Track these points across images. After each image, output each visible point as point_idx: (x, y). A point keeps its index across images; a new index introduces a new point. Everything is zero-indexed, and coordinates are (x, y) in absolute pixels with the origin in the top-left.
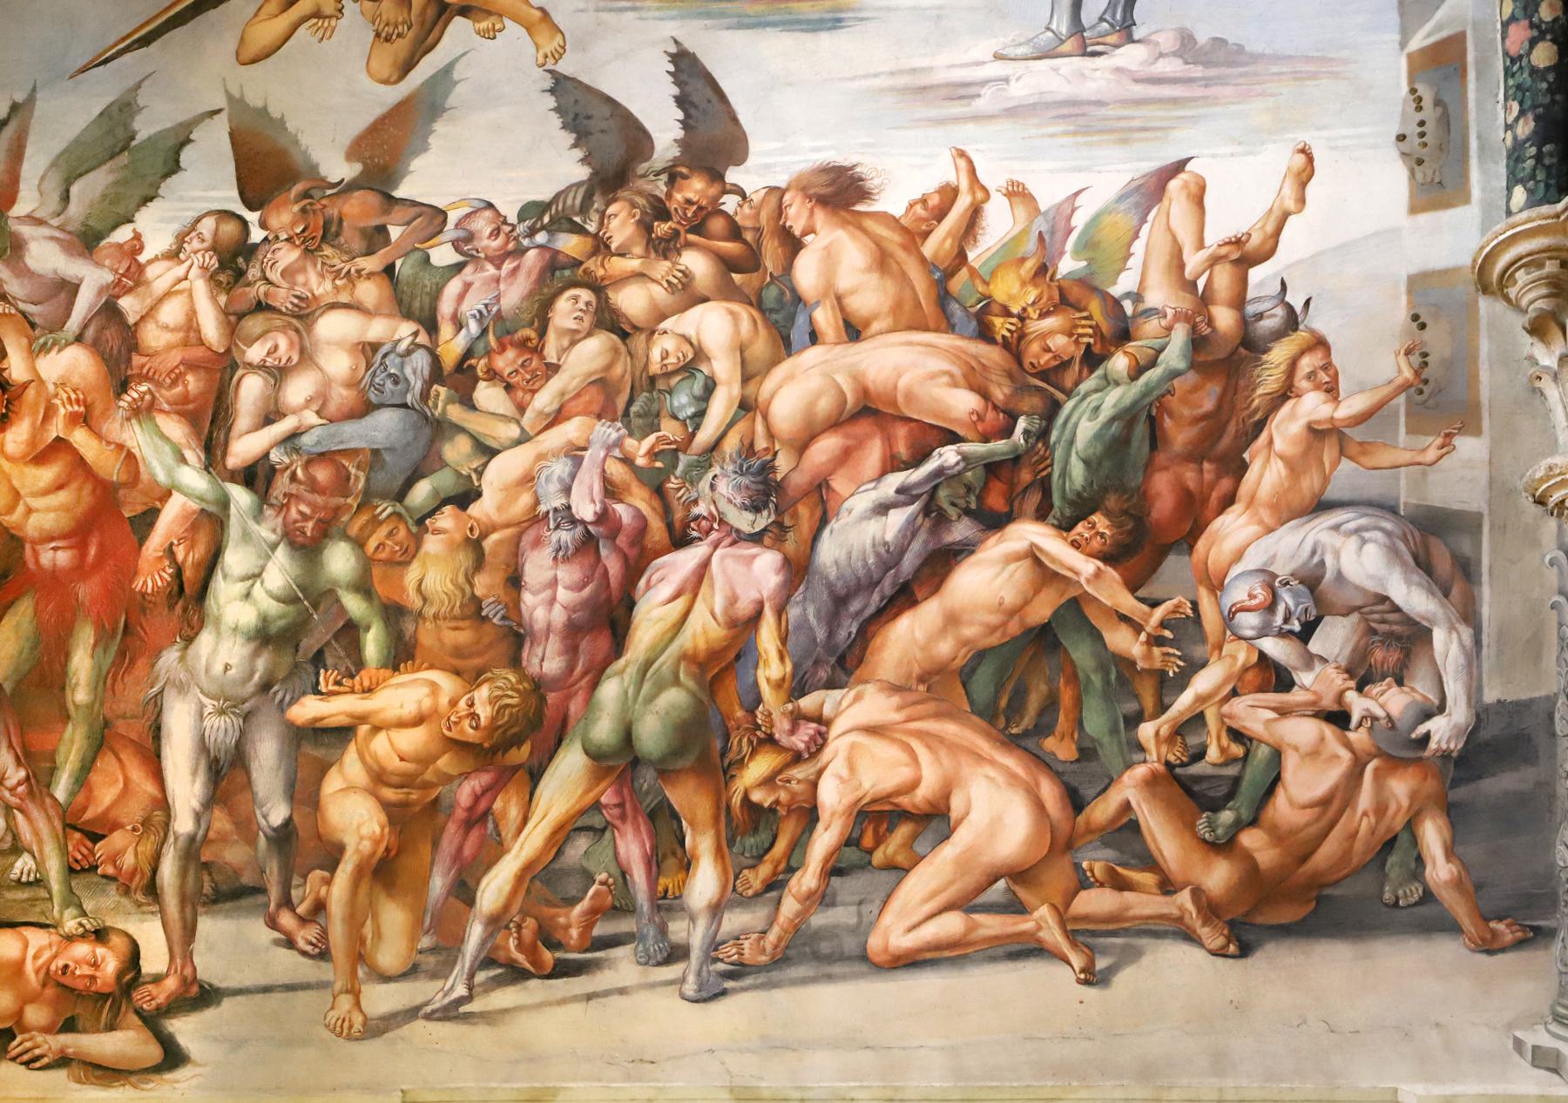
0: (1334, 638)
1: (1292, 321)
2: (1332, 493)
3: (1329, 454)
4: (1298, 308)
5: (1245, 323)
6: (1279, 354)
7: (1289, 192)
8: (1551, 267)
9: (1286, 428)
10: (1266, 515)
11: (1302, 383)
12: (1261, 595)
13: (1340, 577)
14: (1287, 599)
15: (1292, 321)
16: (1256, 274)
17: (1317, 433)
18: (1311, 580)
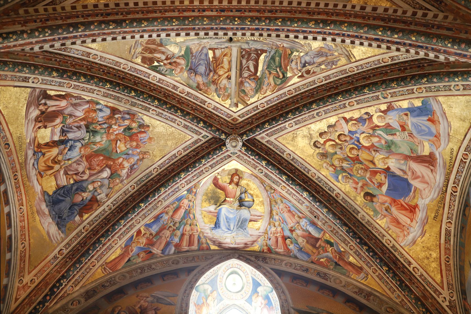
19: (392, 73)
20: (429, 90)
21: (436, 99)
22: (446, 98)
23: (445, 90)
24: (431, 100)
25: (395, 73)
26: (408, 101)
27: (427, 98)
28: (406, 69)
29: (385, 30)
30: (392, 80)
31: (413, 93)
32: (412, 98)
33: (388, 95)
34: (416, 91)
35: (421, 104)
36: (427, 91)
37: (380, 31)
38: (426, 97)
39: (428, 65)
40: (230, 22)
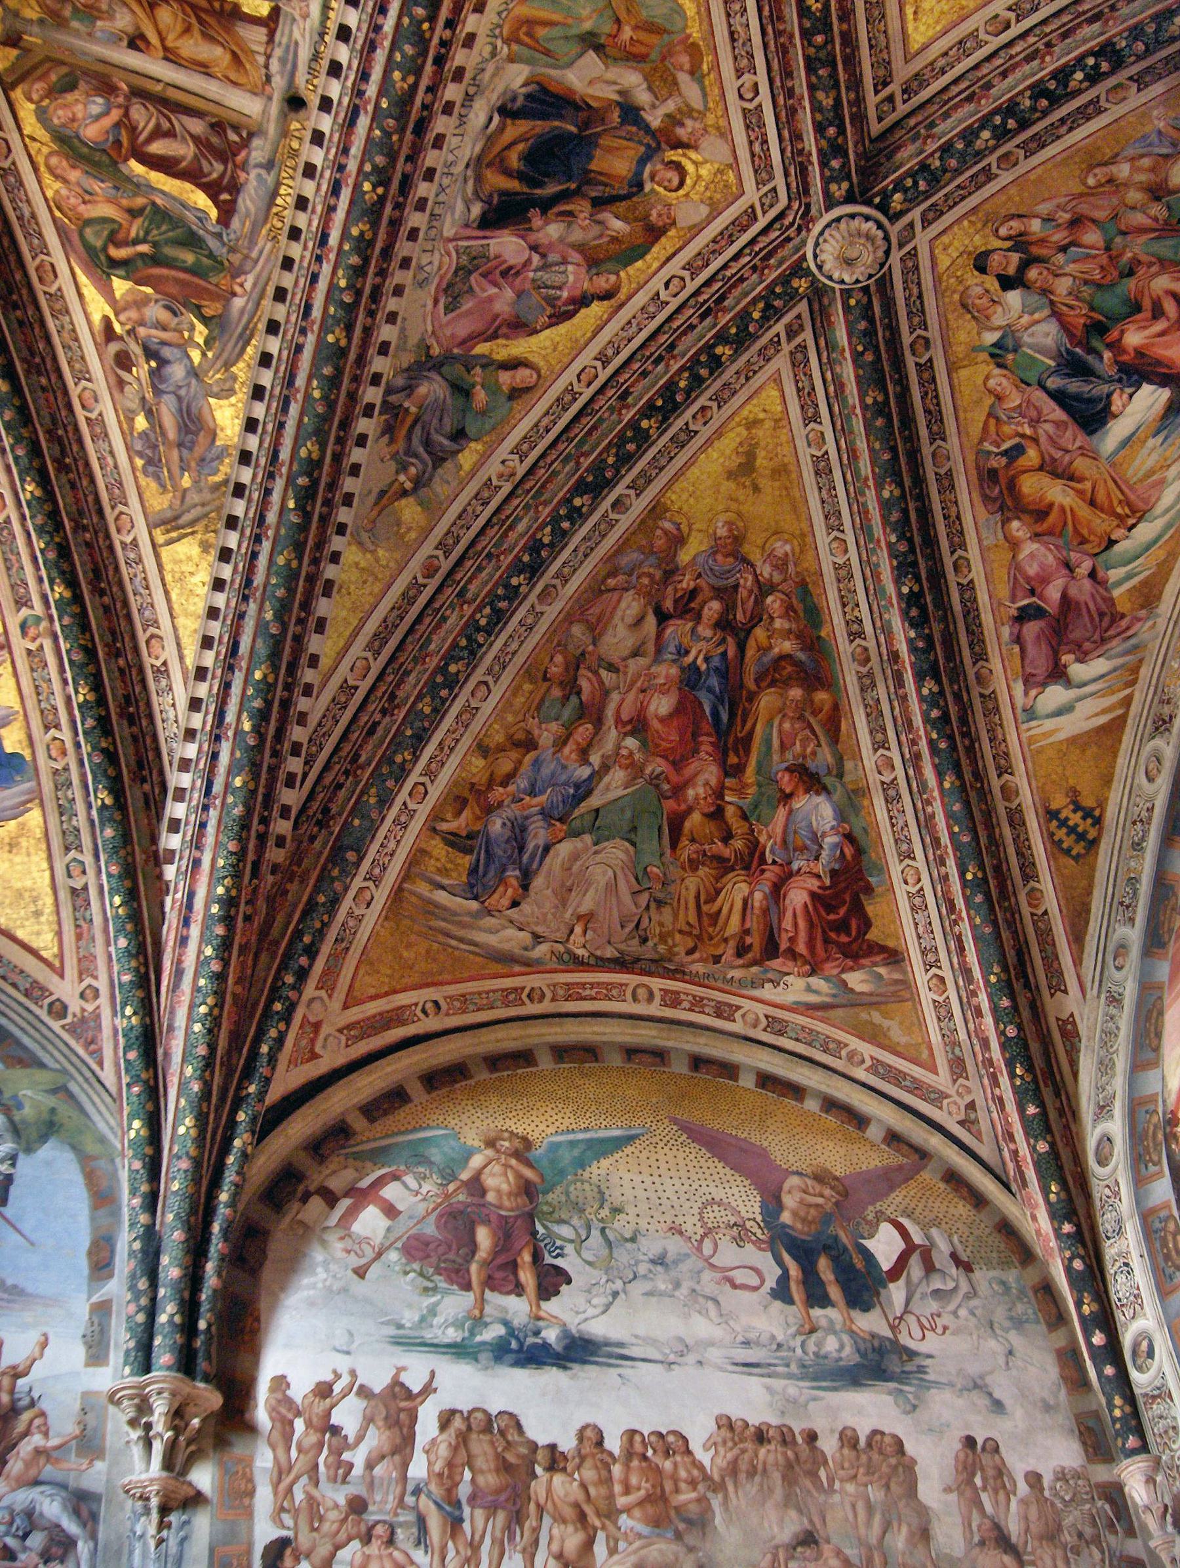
0: (37, 1540)
1: (32, 1404)
2: (42, 1477)
3: (42, 1460)
4: (36, 1397)
5: (14, 1402)
6: (26, 1416)
7: (37, 1350)
8: (136, 1401)
9: (26, 1448)
10: (13, 1483)
11: (34, 1429)
12: (7, 1518)
13: (41, 1514)
14: (18, 1521)
15: (32, 1404)
16: (20, 1382)
17: (38, 1452)
18: (29, 1514)
19: (117, 674)
20: (61, 781)
21: (30, 801)
22: (39, 833)
23: (64, 833)
24: (26, 786)
25: (119, 684)
26: (17, 707)
27: (32, 771)
28: (131, 723)
29: (269, 691)
30: (97, 686)
31: (47, 728)
32: (28, 723)
33: (34, 639)
34: (55, 739)
35: (9, 750)
36: (56, 772)
37: (265, 676)
38: (36, 769)
39: (145, 795)
40: (375, 167)
